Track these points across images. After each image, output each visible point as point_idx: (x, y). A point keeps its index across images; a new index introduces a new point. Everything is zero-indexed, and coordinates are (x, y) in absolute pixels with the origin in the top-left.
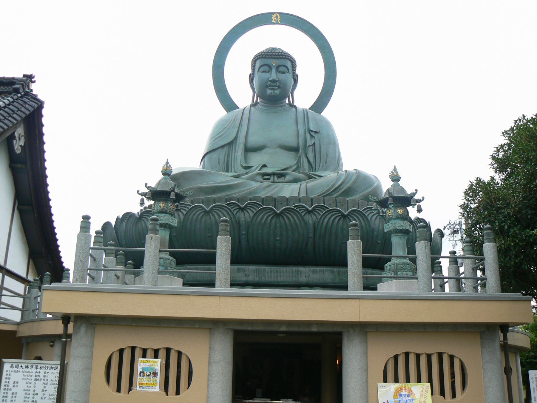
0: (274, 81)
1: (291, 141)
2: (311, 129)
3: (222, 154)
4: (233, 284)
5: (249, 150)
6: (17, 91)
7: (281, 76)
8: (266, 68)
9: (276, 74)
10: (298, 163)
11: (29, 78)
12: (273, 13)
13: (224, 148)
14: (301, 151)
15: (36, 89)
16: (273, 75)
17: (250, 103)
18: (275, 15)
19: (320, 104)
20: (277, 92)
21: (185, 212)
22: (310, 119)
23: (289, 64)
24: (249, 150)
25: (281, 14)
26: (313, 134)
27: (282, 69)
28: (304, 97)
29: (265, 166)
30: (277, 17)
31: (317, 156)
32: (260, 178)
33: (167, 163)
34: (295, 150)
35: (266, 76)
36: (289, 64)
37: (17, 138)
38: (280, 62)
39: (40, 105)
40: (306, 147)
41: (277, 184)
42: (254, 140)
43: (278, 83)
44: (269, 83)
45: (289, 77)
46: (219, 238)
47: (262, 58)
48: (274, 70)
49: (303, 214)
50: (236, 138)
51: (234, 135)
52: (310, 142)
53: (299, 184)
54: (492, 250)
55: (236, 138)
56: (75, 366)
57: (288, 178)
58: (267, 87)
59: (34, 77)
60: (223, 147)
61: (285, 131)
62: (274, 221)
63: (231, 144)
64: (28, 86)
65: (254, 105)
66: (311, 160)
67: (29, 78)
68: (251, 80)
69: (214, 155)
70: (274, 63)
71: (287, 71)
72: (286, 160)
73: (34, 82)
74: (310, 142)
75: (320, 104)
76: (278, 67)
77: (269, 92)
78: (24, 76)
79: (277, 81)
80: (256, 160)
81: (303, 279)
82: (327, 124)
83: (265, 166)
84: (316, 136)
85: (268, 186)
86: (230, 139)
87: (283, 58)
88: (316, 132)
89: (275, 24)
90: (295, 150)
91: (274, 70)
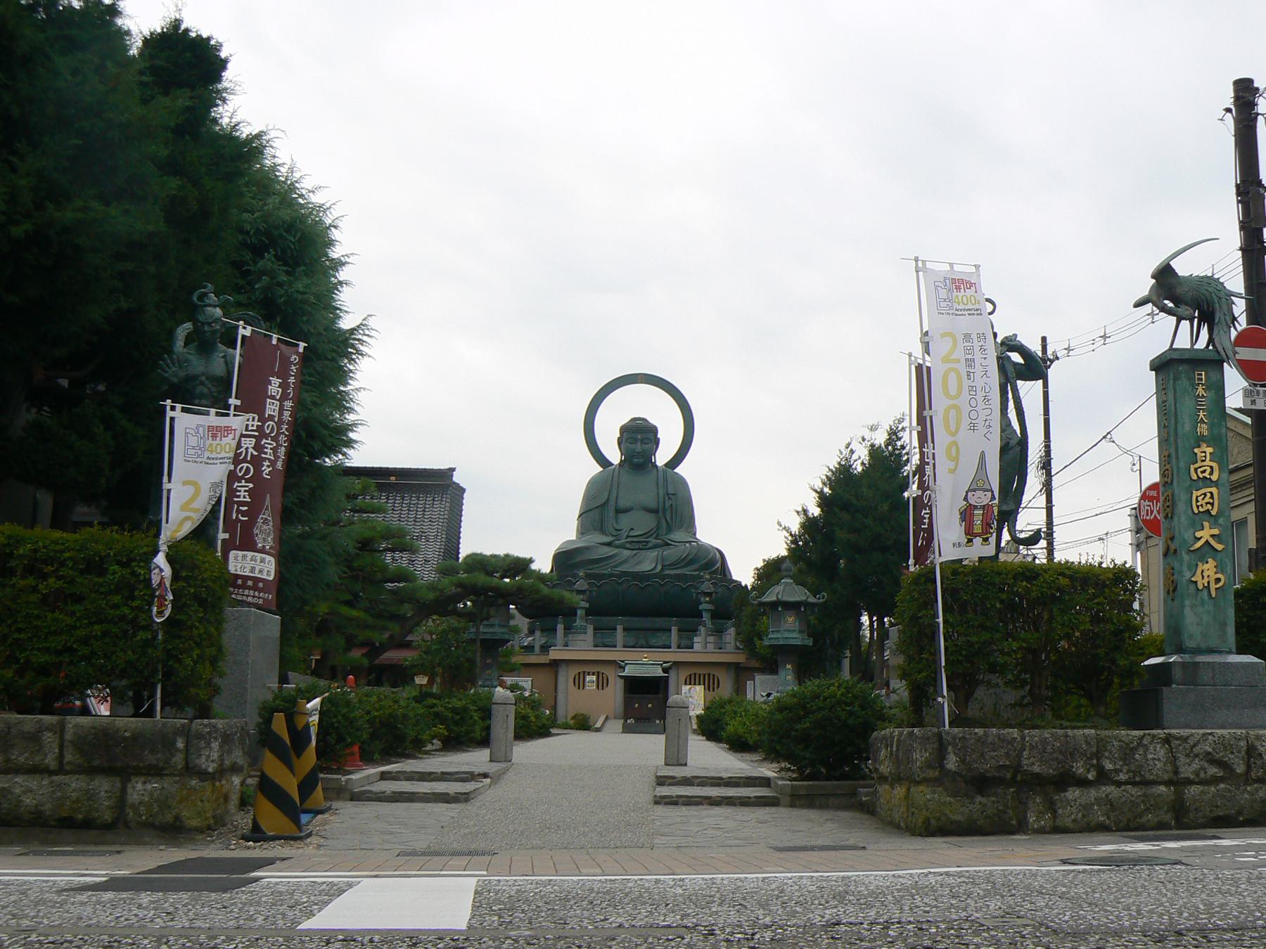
1: (653, 505)
5: (618, 511)
11: (454, 470)
13: (600, 508)
14: (661, 514)
15: (456, 478)
24: (618, 511)
34: (656, 511)
35: (633, 446)
36: (651, 436)
52: (668, 504)
56: (561, 680)
57: (650, 545)
65: (622, 463)
67: (454, 470)
68: (619, 444)
74: (667, 505)
80: (625, 522)
81: (657, 626)
82: (683, 483)
90: (656, 511)
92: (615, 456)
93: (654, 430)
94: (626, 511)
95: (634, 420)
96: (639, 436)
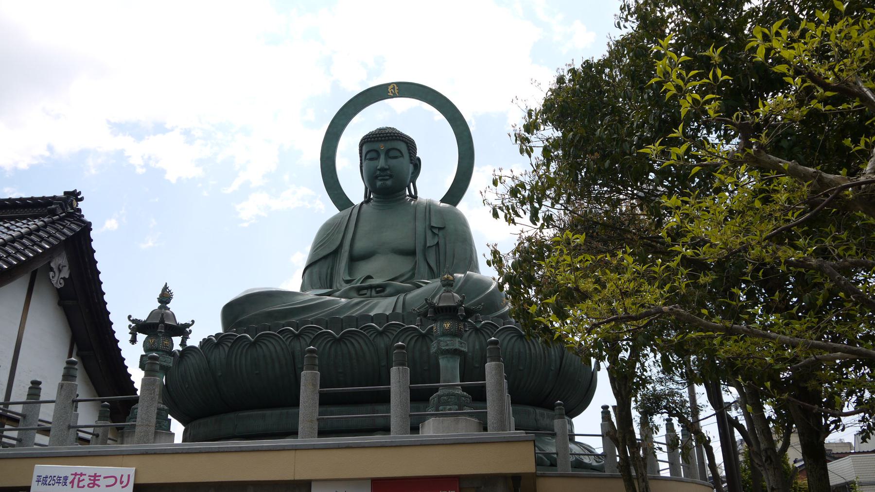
0: (383, 170)
1: (406, 243)
2: (433, 224)
3: (324, 267)
4: (322, 433)
6: (53, 213)
7: (393, 162)
8: (373, 155)
9: (386, 159)
10: (414, 268)
11: (73, 196)
12: (389, 84)
14: (419, 256)
16: (381, 163)
17: (362, 199)
18: (392, 86)
19: (456, 193)
20: (389, 183)
21: (230, 345)
22: (432, 213)
23: (403, 147)
24: (354, 259)
25: (398, 84)
26: (436, 231)
27: (392, 154)
28: (431, 186)
29: (369, 277)
30: (394, 88)
31: (442, 258)
32: (353, 294)
33: (166, 288)
34: (412, 253)
35: (373, 163)
36: (403, 147)
37: (56, 270)
38: (390, 145)
39: (87, 227)
40: (426, 249)
41: (375, 301)
42: (361, 245)
43: (389, 172)
44: (378, 172)
45: (404, 163)
46: (394, 370)
47: (371, 141)
48: (382, 157)
49: (371, 338)
50: (341, 245)
51: (338, 243)
52: (431, 242)
53: (394, 299)
54: (493, 372)
55: (341, 245)
57: (388, 290)
58: (376, 177)
59: (80, 193)
60: (325, 258)
61: (398, 231)
62: (333, 349)
63: (336, 253)
64: (71, 206)
65: (367, 200)
66: (433, 264)
67: (73, 196)
69: (316, 269)
70: (382, 147)
71: (398, 154)
72: (403, 265)
73: (81, 199)
75: (456, 193)
76: (387, 152)
77: (379, 183)
78: (66, 193)
79: (386, 170)
83: (369, 277)
84: (441, 234)
85: (357, 304)
86: (334, 247)
87: (393, 140)
88: (440, 229)
89: (392, 97)
90: (412, 253)
91: (382, 157)
92: (355, 189)
93: (410, 145)
94: (367, 256)
95: (380, 129)
96: (391, 159)
